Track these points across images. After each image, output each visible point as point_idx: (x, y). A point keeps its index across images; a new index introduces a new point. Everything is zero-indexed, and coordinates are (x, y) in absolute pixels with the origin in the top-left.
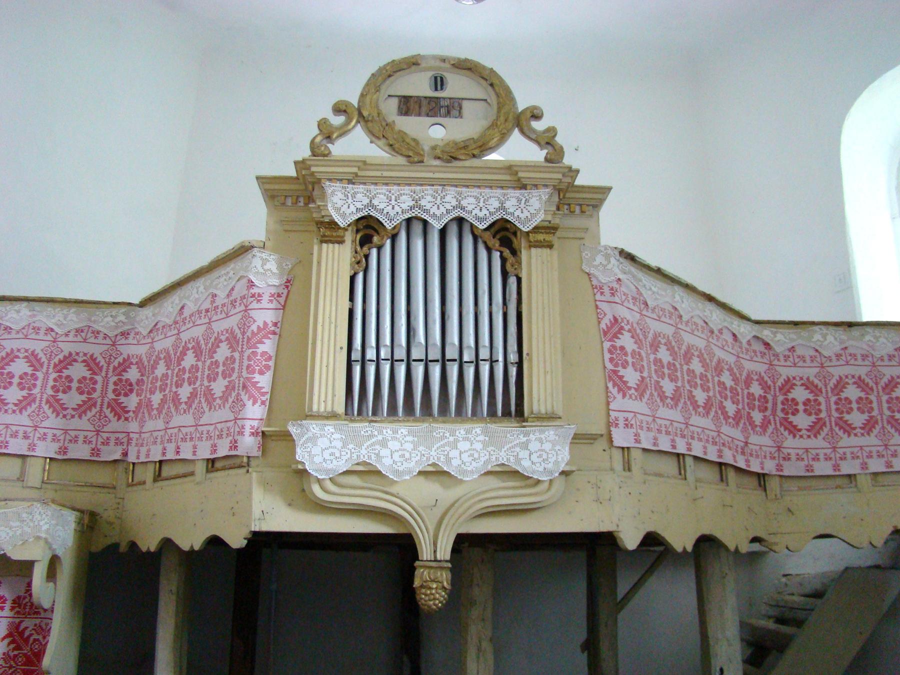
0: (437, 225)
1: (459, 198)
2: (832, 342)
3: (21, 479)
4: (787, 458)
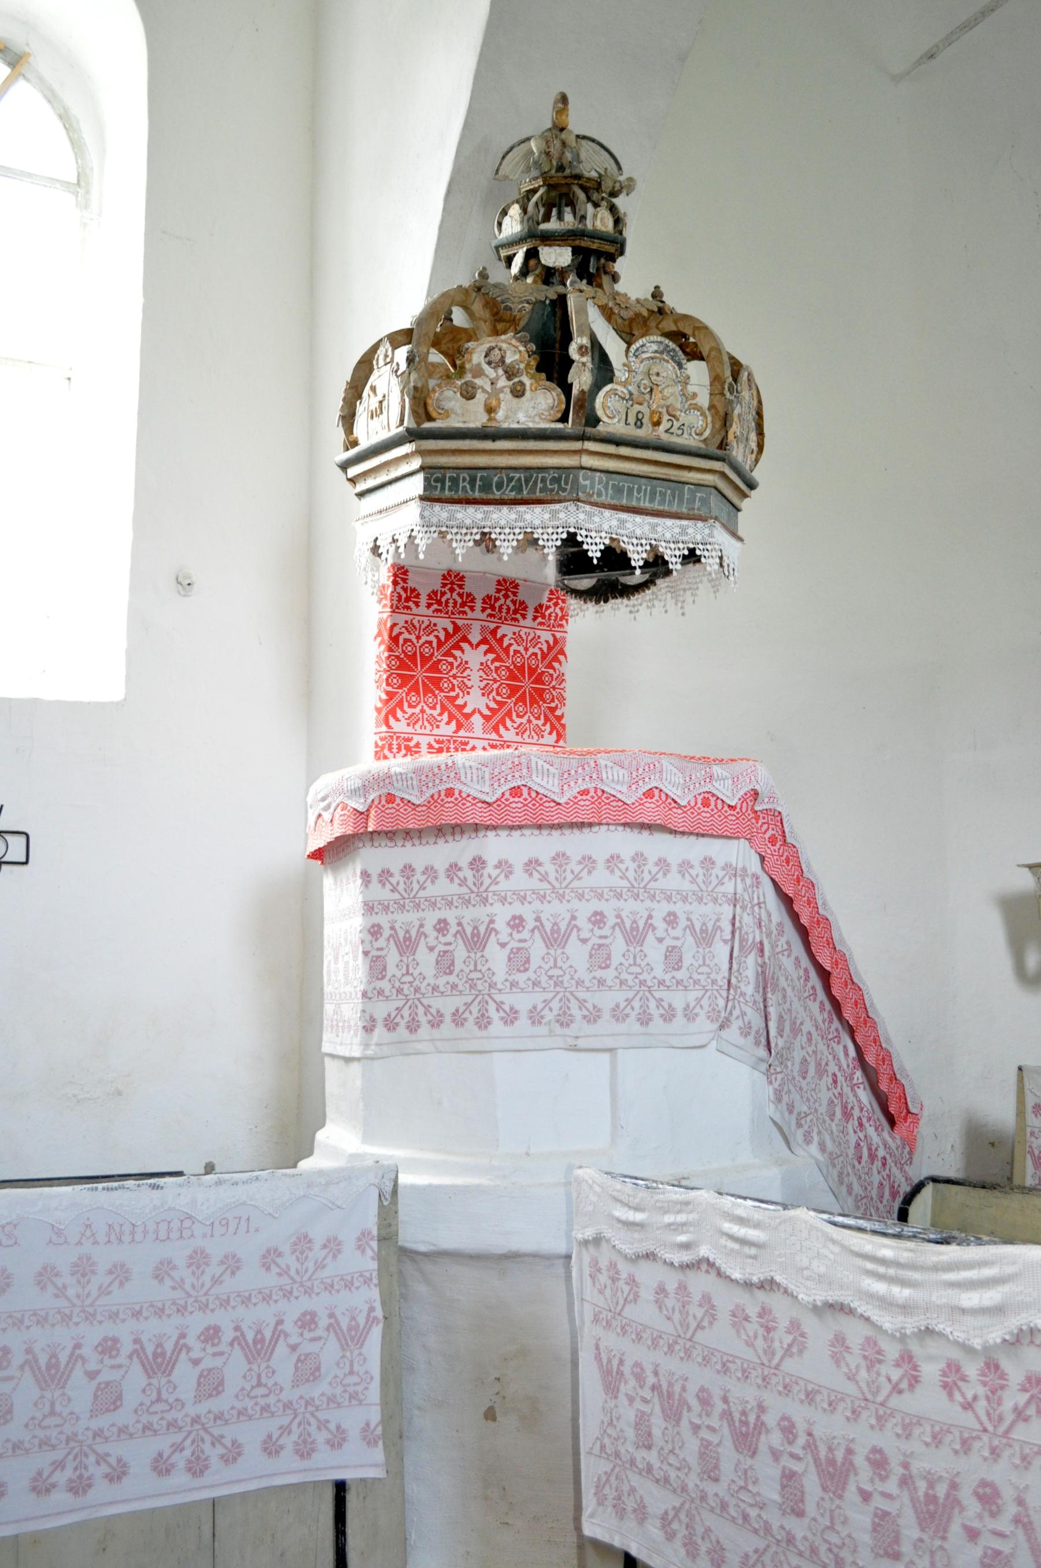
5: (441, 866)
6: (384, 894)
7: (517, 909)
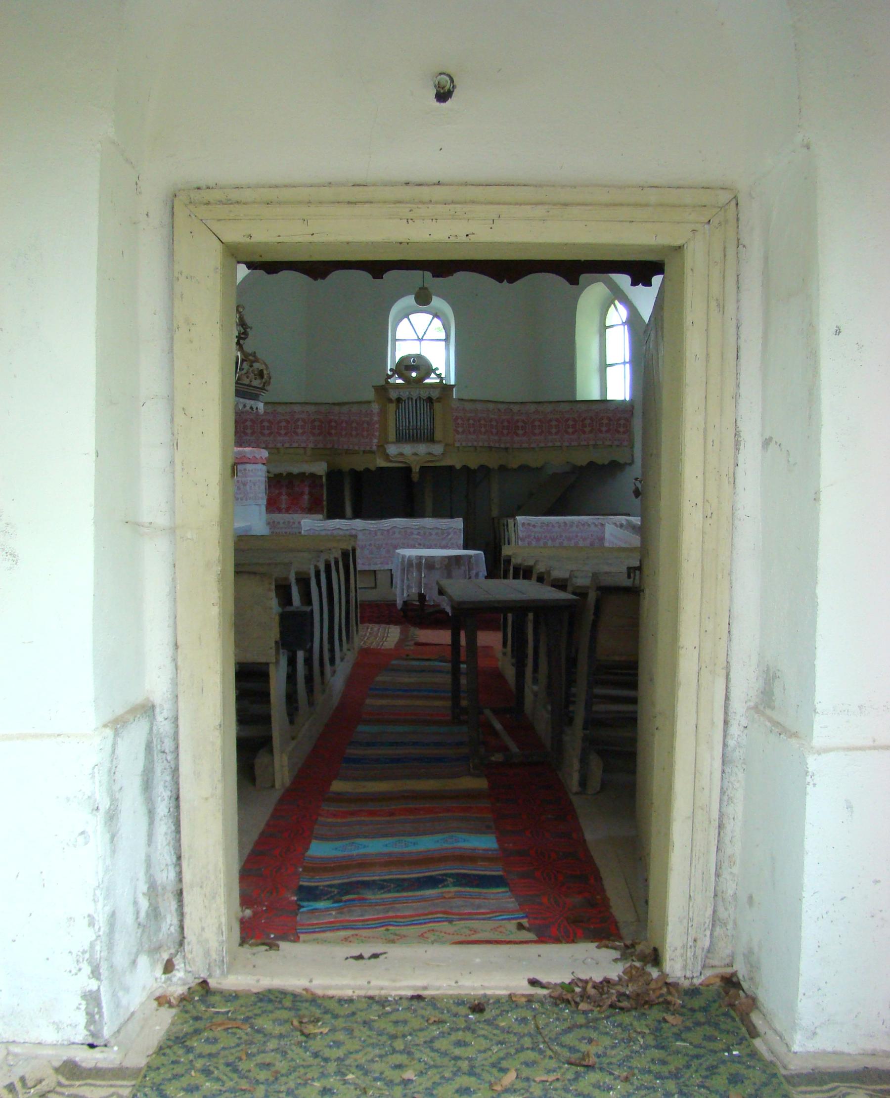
0: (414, 399)
3: (305, 453)
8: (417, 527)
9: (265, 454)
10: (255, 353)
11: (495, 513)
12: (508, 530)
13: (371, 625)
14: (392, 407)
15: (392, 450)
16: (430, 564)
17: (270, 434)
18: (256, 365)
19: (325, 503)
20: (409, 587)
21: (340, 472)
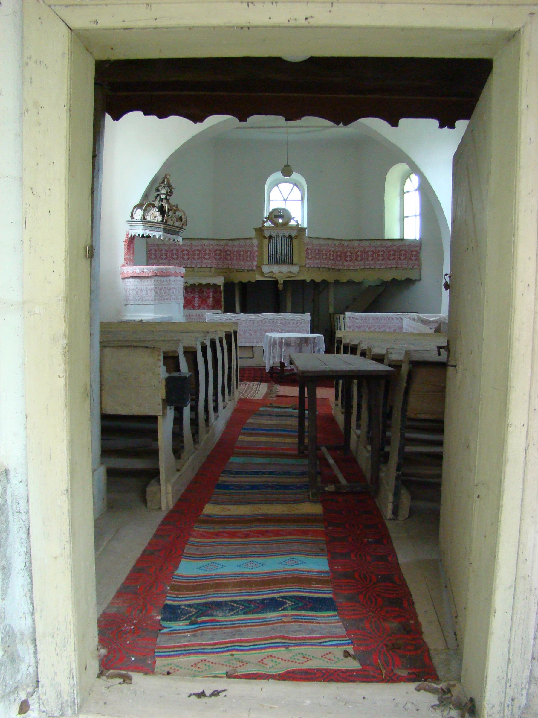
0: (280, 236)
1: (284, 232)
2: (356, 244)
3: (210, 271)
4: (344, 266)
5: (165, 280)
6: (157, 283)
7: (173, 286)
8: (281, 318)
9: (183, 270)
10: (177, 205)
11: (331, 310)
12: (339, 322)
13: (248, 383)
14: (266, 241)
15: (266, 269)
16: (288, 343)
17: (188, 259)
18: (178, 213)
19: (222, 303)
20: (274, 358)
21: (233, 284)
